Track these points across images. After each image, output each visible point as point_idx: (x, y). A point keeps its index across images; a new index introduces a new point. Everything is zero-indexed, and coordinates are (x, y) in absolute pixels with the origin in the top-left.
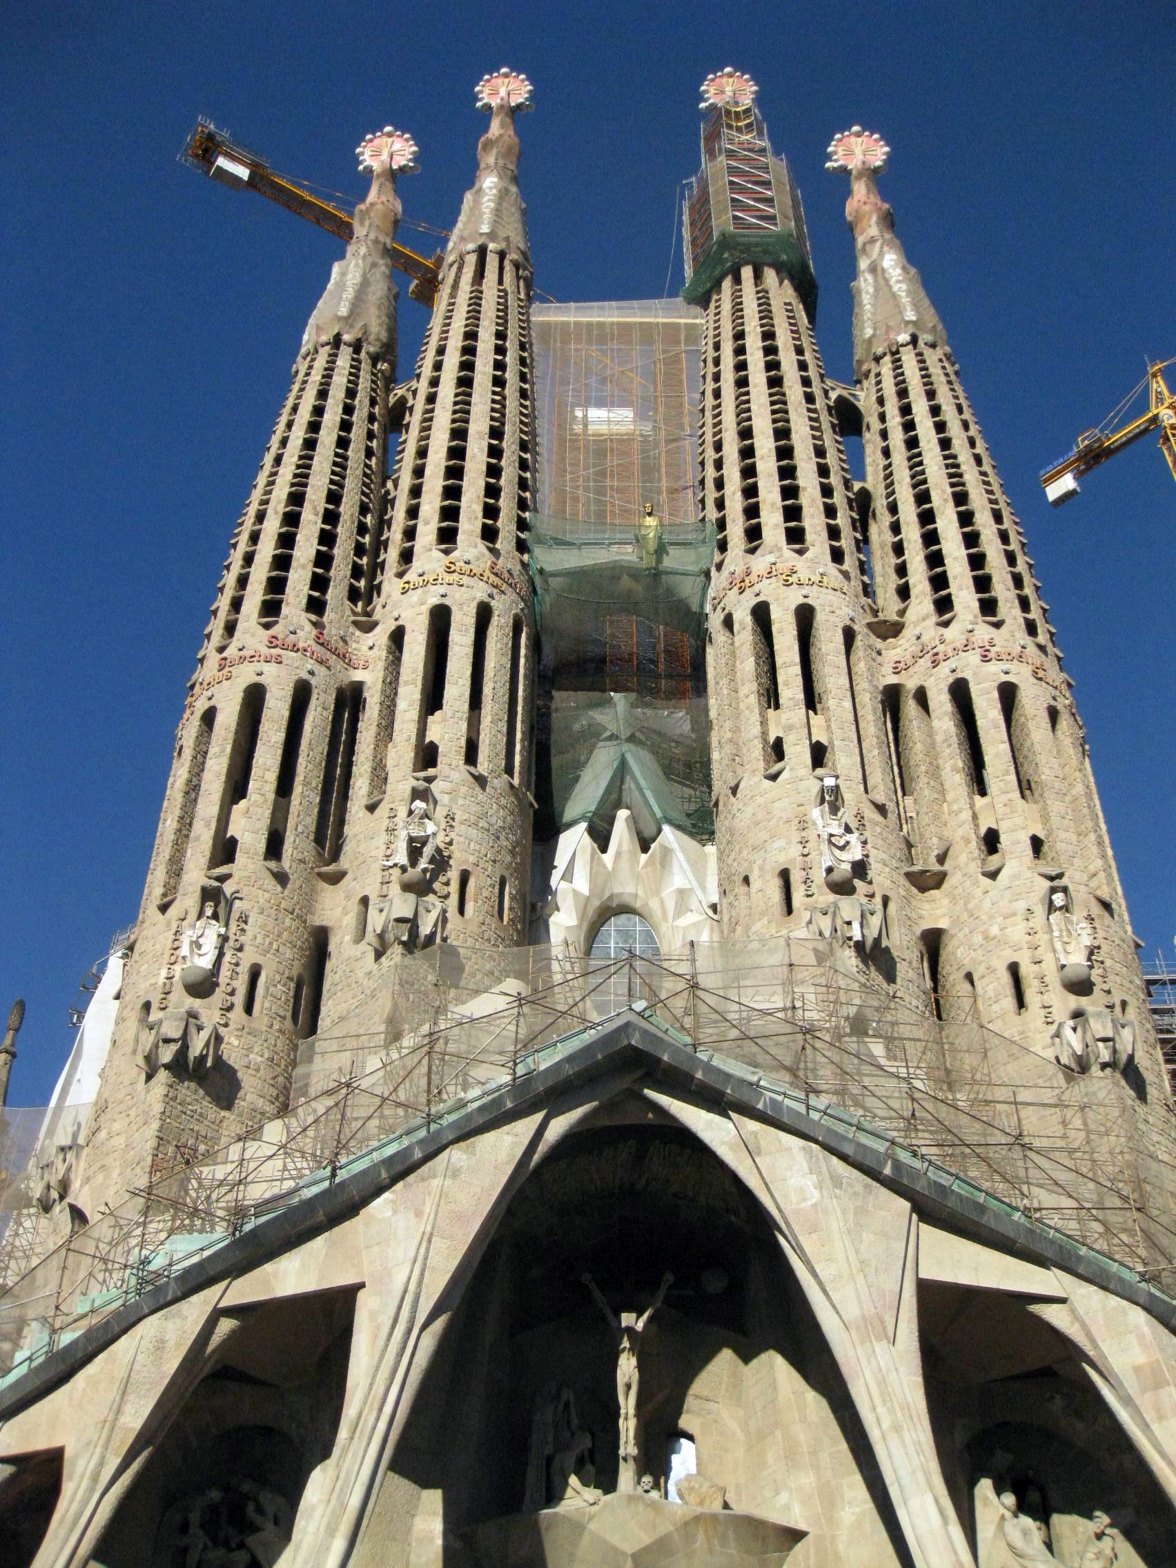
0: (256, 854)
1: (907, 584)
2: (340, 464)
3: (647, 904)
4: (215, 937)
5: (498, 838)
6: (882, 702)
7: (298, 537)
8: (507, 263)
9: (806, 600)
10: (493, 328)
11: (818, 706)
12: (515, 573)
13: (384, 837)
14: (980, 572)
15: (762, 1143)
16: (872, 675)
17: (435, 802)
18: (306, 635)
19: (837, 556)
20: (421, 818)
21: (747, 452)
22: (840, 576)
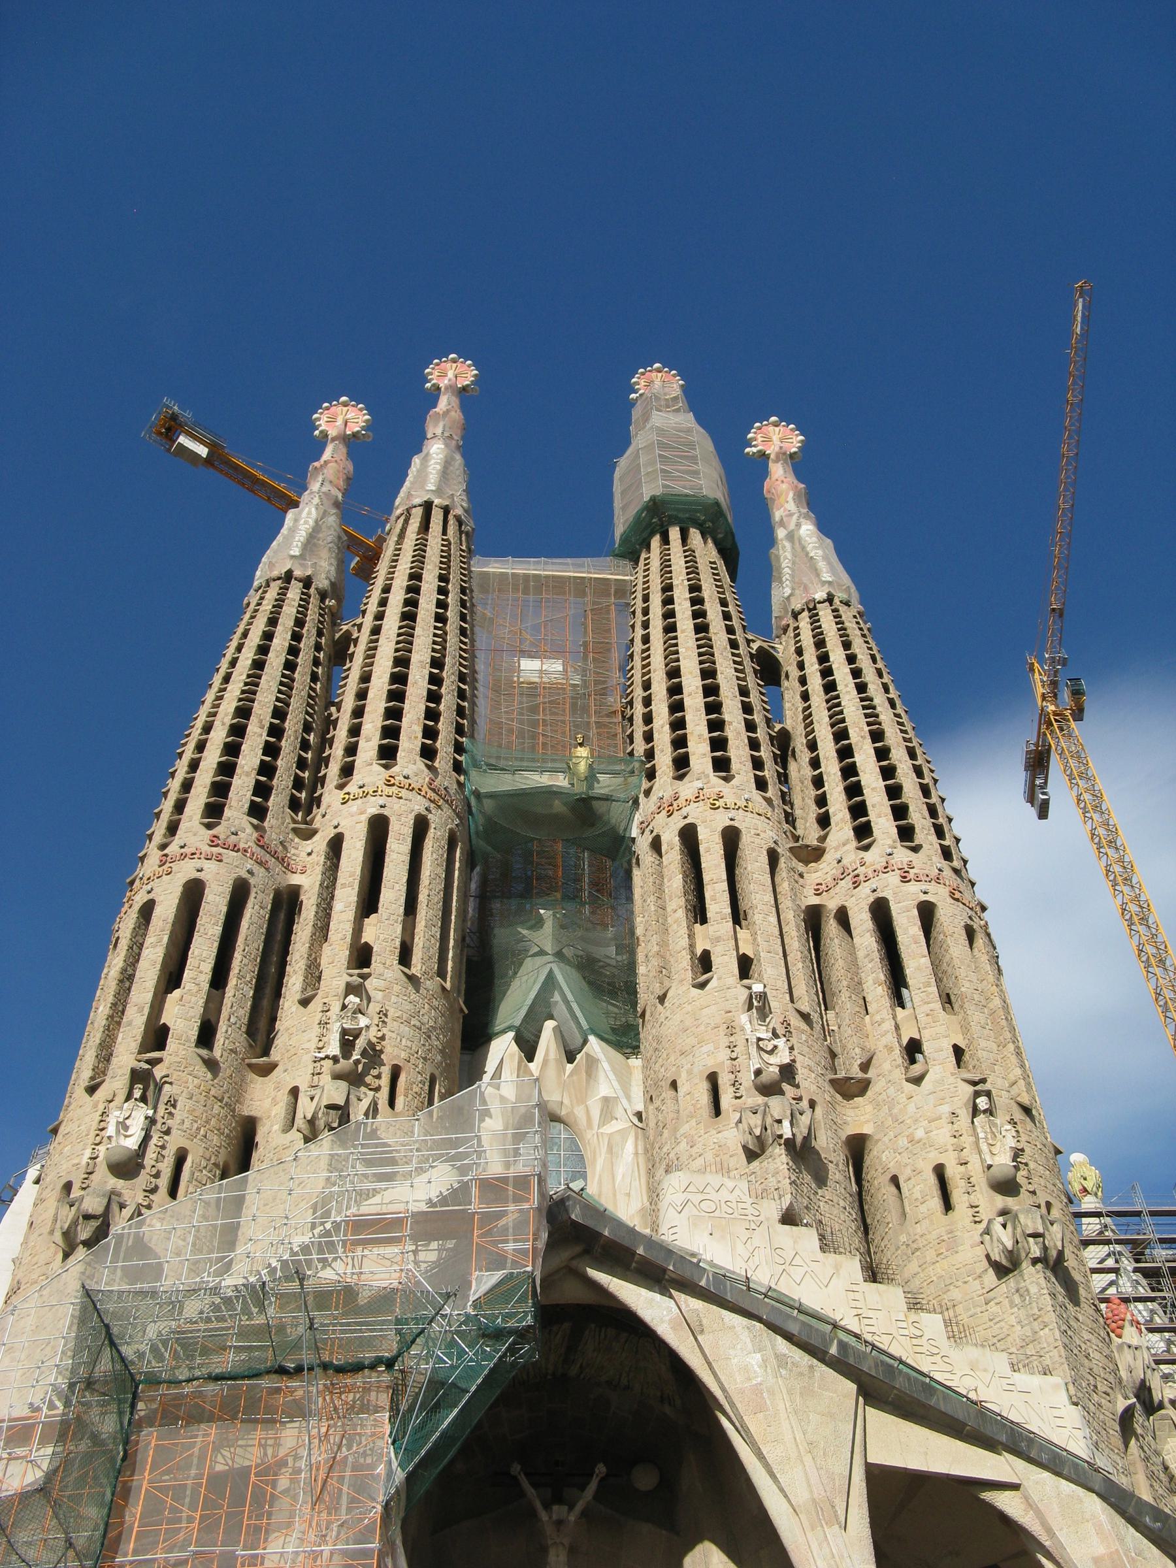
0: (188, 1040)
1: (827, 811)
2: (287, 684)
4: (142, 1118)
5: (429, 1037)
6: (805, 920)
8: (450, 517)
9: (732, 823)
10: (437, 572)
11: (743, 923)
12: (452, 792)
13: (317, 1030)
14: (898, 801)
15: (704, 1321)
17: (369, 999)
18: (247, 837)
19: (761, 784)
20: (354, 1013)
21: (675, 690)
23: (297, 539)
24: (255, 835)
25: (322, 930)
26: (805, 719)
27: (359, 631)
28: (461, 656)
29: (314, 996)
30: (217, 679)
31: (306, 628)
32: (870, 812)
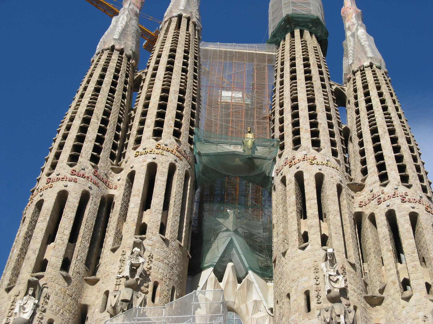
0: (57, 267)
1: (366, 167)
2: (110, 100)
3: (240, 307)
4: (32, 304)
5: (172, 268)
6: (354, 219)
7: (88, 129)
8: (191, 22)
9: (320, 171)
10: (183, 49)
11: (324, 219)
12: (187, 153)
13: (119, 264)
14: (401, 163)
16: (349, 206)
17: (144, 250)
19: (335, 153)
20: (137, 256)
21: (295, 107)
22: (336, 162)
23: (117, 30)
24: (93, 170)
25: (123, 216)
26: (357, 123)
27: (146, 75)
28: (194, 89)
29: (119, 247)
30: (77, 96)
31: (120, 73)
32: (387, 168)
